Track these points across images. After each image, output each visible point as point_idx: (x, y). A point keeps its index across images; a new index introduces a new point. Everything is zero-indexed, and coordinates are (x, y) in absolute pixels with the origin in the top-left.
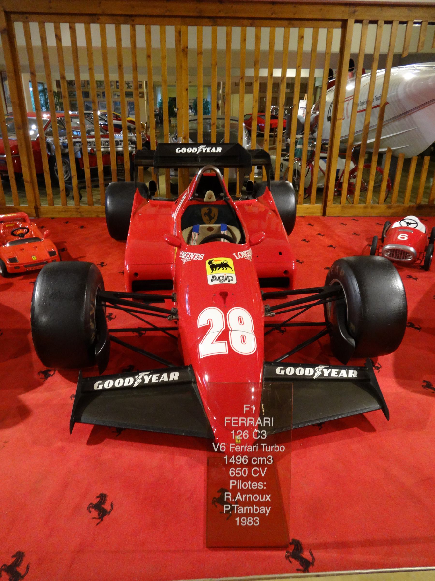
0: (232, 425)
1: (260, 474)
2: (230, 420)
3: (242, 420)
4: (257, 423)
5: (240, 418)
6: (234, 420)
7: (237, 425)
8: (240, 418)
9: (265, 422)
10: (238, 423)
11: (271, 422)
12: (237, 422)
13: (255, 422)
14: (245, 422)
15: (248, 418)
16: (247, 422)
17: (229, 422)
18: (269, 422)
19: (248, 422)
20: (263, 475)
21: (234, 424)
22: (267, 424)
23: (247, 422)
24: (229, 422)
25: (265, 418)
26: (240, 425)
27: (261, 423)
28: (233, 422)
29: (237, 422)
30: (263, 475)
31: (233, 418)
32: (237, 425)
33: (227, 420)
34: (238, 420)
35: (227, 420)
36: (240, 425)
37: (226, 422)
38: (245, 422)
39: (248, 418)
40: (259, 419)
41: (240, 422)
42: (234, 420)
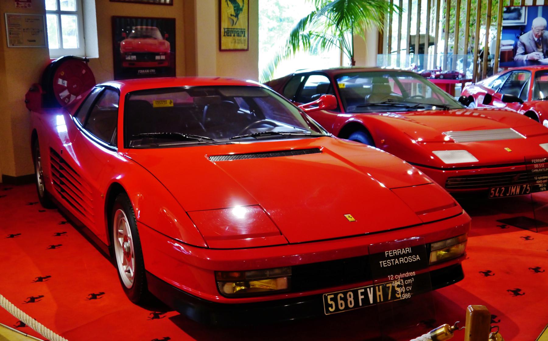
0: (390, 256)
1: (410, 289)
2: (388, 253)
3: (395, 252)
4: (403, 252)
5: (393, 251)
6: (391, 252)
7: (392, 255)
8: (393, 251)
9: (406, 251)
10: (392, 254)
11: (410, 250)
12: (392, 253)
13: (402, 252)
14: (396, 253)
15: (398, 250)
16: (397, 252)
17: (388, 254)
18: (408, 250)
19: (398, 252)
20: (410, 289)
21: (391, 254)
22: (408, 252)
23: (397, 252)
24: (388, 254)
25: (406, 249)
26: (394, 255)
27: (404, 252)
28: (390, 253)
29: (392, 253)
30: (410, 289)
31: (390, 251)
32: (392, 255)
33: (387, 253)
34: (392, 252)
35: (387, 253)
37: (386, 254)
38: (396, 253)
39: (398, 250)
40: (403, 249)
41: (394, 253)
42: (391, 252)
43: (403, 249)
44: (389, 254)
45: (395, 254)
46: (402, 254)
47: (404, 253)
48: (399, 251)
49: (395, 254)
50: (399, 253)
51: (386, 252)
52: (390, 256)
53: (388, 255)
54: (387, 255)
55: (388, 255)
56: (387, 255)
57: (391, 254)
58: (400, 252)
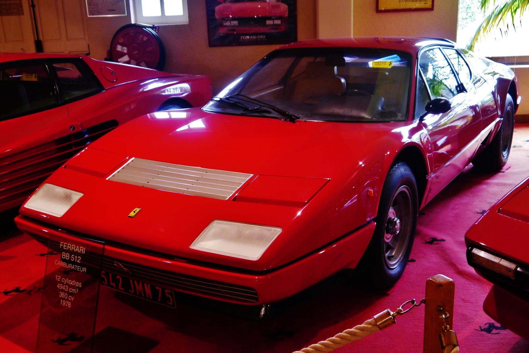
0: (64, 248)
4: (77, 250)
5: (69, 244)
6: (65, 245)
7: (66, 249)
9: (80, 250)
11: (84, 250)
12: (66, 246)
19: (72, 248)
21: (65, 247)
26: (68, 249)
28: (65, 246)
31: (65, 243)
32: (66, 249)
33: (62, 244)
34: (67, 245)
35: (62, 244)
36: (68, 249)
37: (61, 245)
38: (70, 247)
39: (73, 245)
40: (78, 247)
41: (68, 247)
42: (65, 245)
43: (78, 247)
44: (64, 246)
45: (69, 248)
46: (75, 252)
47: (77, 251)
49: (69, 248)
52: (64, 248)
54: (62, 246)
55: (62, 247)
56: (62, 246)
57: (65, 247)
58: (74, 248)
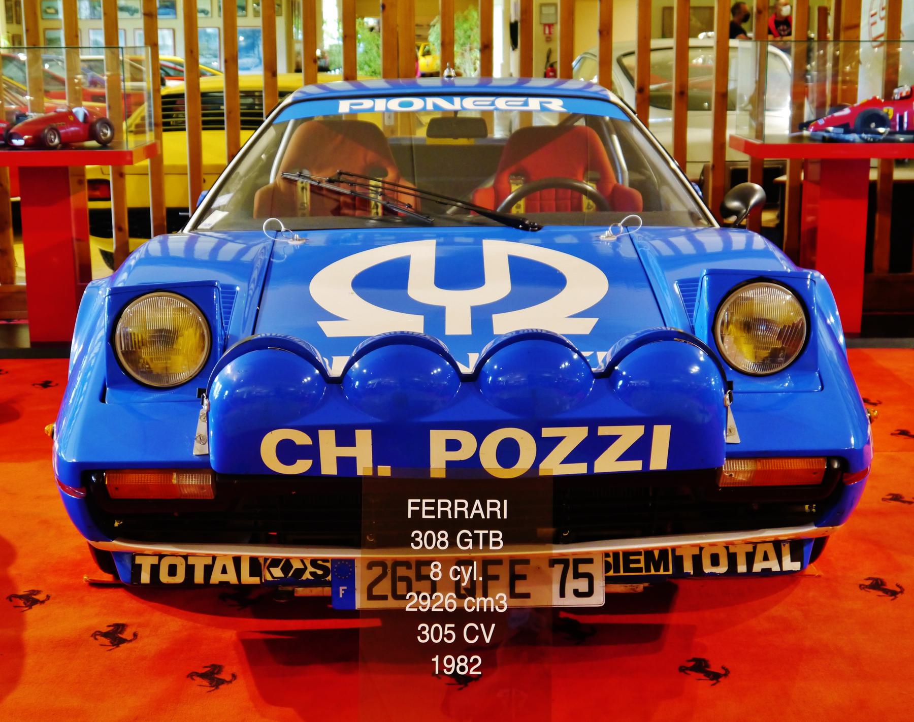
2: (420, 505)
3: (444, 505)
4: (474, 511)
6: (427, 504)
9: (489, 509)
11: (502, 509)
15: (456, 501)
16: (452, 509)
19: (457, 509)
21: (428, 513)
22: (493, 514)
23: (452, 509)
26: (439, 516)
28: (424, 508)
31: (424, 501)
33: (413, 504)
34: (435, 505)
35: (413, 504)
38: (448, 509)
39: (456, 501)
40: (478, 502)
41: (440, 509)
43: (478, 502)
45: (444, 513)
48: (461, 505)
50: (461, 513)
51: (410, 501)
52: (424, 516)
53: (416, 514)
57: (428, 513)
58: (465, 509)
